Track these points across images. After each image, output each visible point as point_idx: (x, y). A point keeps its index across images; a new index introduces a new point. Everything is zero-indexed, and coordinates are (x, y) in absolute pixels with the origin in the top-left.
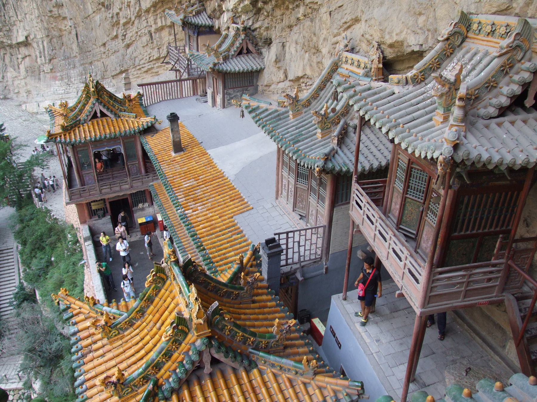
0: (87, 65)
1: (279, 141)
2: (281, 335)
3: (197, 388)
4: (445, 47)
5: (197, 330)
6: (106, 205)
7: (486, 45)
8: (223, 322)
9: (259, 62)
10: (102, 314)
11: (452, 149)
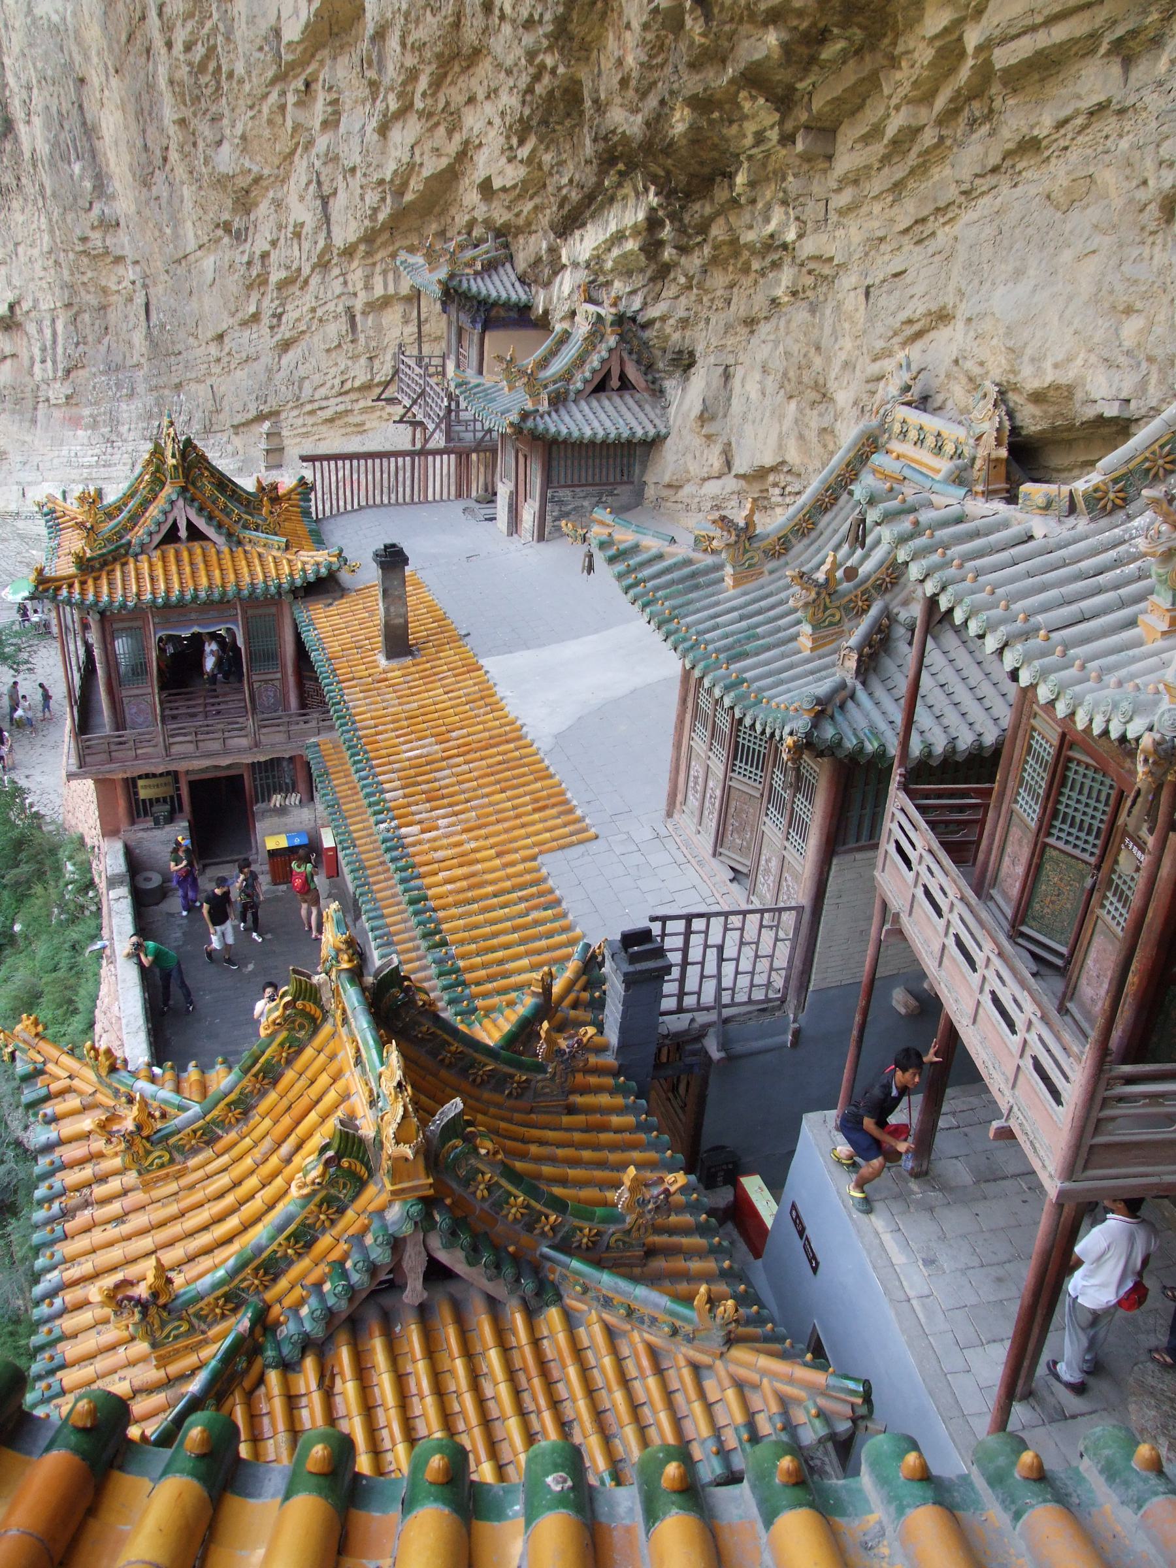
0: (167, 392)
2: (641, 1215)
3: (378, 1348)
5: (395, 1174)
8: (472, 1161)
9: (652, 415)
10: (131, 1101)
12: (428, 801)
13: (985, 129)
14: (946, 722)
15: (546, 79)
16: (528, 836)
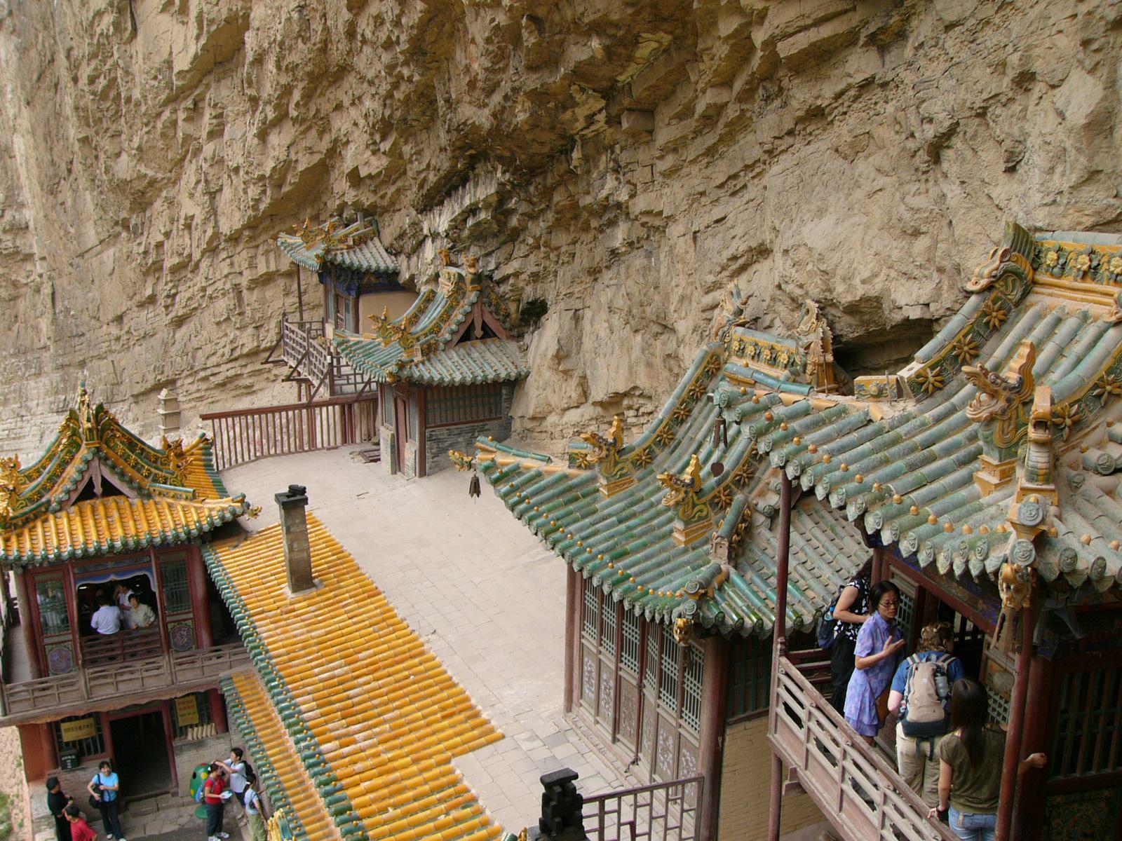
0: (72, 370)
4: (987, 306)
7: (1083, 300)
13: (777, 103)
15: (404, 87)
16: (439, 742)
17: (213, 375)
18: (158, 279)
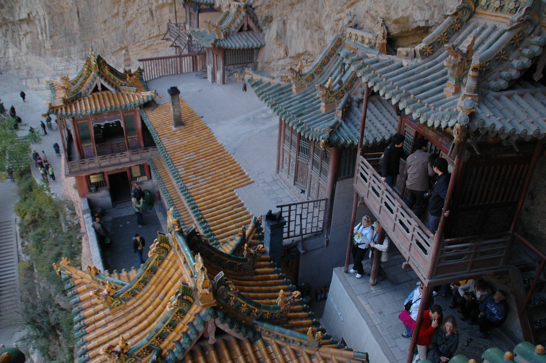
1: (282, 114)
2: (286, 306)
4: (454, 22)
5: (202, 300)
6: (104, 178)
7: (494, 20)
8: (228, 293)
10: (104, 284)
11: (468, 117)
12: (194, 174)
14: (372, 132)
17: (142, 44)
18: (119, 6)
